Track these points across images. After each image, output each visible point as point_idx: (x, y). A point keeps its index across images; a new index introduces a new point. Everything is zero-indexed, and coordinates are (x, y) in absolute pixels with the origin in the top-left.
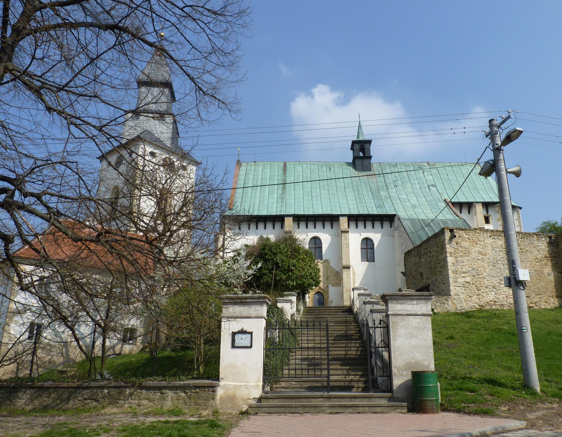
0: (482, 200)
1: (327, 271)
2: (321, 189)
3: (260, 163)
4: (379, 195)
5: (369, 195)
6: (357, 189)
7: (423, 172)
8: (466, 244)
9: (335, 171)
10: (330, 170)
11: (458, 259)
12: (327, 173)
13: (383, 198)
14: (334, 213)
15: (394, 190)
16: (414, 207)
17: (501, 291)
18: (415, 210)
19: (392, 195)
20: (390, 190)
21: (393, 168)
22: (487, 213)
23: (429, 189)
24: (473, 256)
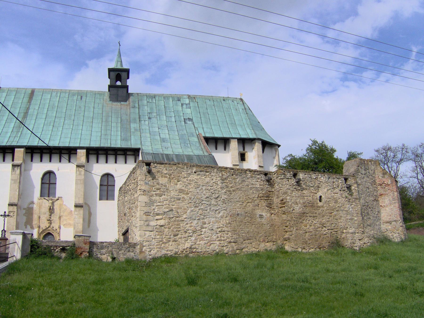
0: (238, 136)
1: (60, 210)
2: (66, 119)
4: (129, 127)
5: (117, 127)
6: (107, 121)
7: (182, 105)
8: (163, 181)
9: (87, 101)
10: (81, 99)
11: (153, 198)
12: (78, 102)
13: (133, 130)
14: (72, 145)
15: (147, 123)
16: (163, 140)
17: (203, 236)
18: (163, 144)
19: (143, 127)
20: (143, 122)
21: (150, 100)
22: (244, 150)
23: (185, 123)
24: (173, 193)
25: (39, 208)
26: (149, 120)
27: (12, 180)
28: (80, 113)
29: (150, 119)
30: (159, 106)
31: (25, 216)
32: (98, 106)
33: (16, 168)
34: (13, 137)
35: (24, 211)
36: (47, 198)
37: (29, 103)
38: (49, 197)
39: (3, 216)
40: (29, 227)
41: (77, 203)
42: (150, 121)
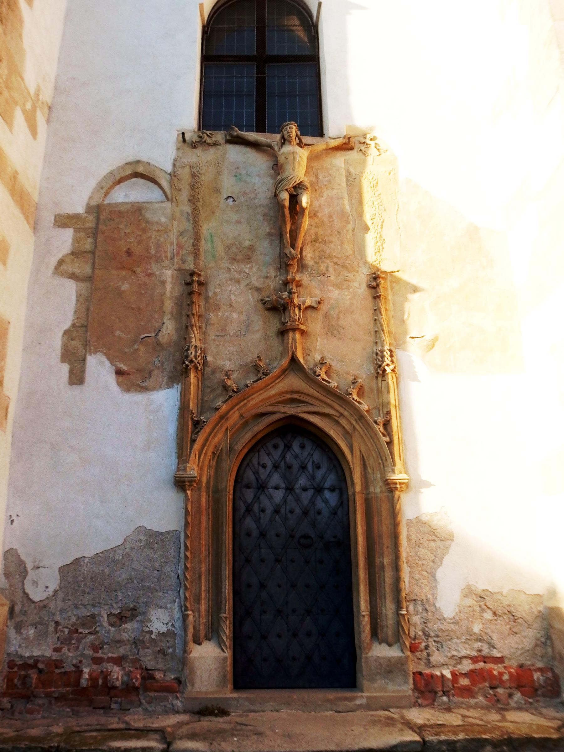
25: (187, 209)
31: (72, 276)
38: (261, 129)
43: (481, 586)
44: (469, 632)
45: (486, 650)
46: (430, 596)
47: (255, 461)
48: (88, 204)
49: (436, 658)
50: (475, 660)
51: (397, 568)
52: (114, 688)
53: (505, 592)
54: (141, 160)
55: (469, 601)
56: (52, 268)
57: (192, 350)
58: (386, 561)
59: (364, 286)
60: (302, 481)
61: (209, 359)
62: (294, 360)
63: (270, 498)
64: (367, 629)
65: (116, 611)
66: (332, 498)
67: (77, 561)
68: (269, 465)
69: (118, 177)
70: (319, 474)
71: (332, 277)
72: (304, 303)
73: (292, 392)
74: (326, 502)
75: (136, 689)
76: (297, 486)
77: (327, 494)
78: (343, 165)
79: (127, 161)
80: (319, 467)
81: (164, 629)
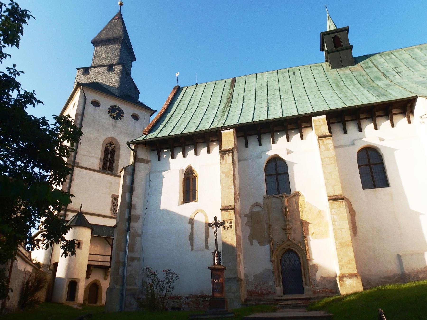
3: (202, 84)
5: (357, 88)
6: (337, 86)
10: (294, 74)
13: (383, 86)
14: (302, 112)
26: (399, 74)
27: (222, 172)
28: (298, 86)
29: (400, 73)
30: (404, 59)
31: (248, 226)
32: (319, 76)
33: (226, 156)
34: (218, 121)
35: (246, 219)
36: (277, 196)
37: (231, 90)
38: (279, 194)
39: (213, 225)
40: (255, 242)
41: (332, 195)
42: (402, 75)
43: (324, 276)
44: (322, 284)
45: (325, 286)
46: (315, 278)
47: (284, 257)
48: (249, 212)
49: (317, 288)
50: (323, 288)
51: (309, 274)
52: (264, 294)
53: (328, 277)
54: (257, 202)
55: (322, 279)
56: (245, 225)
57: (271, 238)
58: (307, 272)
59: (300, 224)
60: (292, 259)
61: (274, 239)
62: (288, 239)
63: (287, 263)
64: (305, 284)
65: (263, 282)
66: (298, 262)
67: (256, 274)
68: (286, 257)
69: (254, 206)
70: (295, 258)
71: (294, 223)
72: (289, 228)
73: (289, 244)
74: (297, 263)
75: (268, 294)
76: (291, 261)
77: (297, 262)
78: (294, 200)
79: (255, 203)
80: (295, 257)
81: (271, 285)
